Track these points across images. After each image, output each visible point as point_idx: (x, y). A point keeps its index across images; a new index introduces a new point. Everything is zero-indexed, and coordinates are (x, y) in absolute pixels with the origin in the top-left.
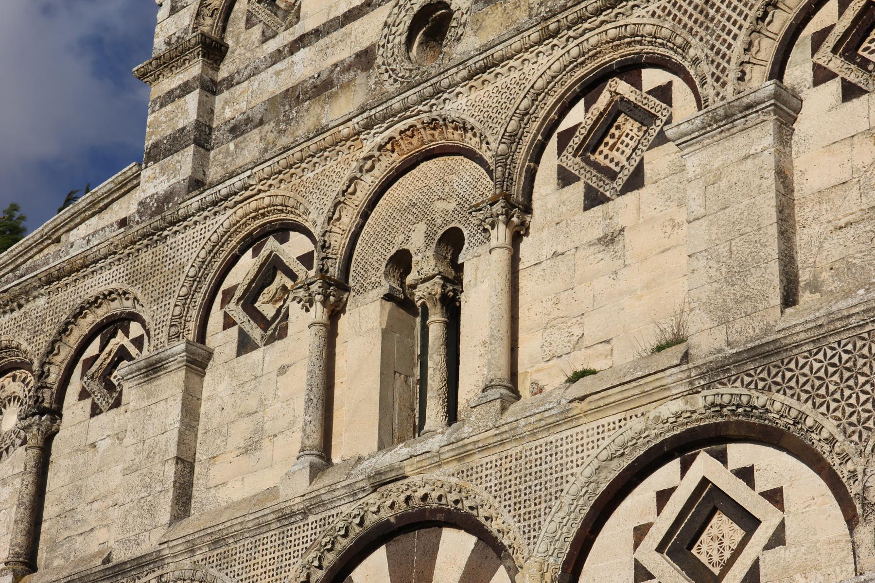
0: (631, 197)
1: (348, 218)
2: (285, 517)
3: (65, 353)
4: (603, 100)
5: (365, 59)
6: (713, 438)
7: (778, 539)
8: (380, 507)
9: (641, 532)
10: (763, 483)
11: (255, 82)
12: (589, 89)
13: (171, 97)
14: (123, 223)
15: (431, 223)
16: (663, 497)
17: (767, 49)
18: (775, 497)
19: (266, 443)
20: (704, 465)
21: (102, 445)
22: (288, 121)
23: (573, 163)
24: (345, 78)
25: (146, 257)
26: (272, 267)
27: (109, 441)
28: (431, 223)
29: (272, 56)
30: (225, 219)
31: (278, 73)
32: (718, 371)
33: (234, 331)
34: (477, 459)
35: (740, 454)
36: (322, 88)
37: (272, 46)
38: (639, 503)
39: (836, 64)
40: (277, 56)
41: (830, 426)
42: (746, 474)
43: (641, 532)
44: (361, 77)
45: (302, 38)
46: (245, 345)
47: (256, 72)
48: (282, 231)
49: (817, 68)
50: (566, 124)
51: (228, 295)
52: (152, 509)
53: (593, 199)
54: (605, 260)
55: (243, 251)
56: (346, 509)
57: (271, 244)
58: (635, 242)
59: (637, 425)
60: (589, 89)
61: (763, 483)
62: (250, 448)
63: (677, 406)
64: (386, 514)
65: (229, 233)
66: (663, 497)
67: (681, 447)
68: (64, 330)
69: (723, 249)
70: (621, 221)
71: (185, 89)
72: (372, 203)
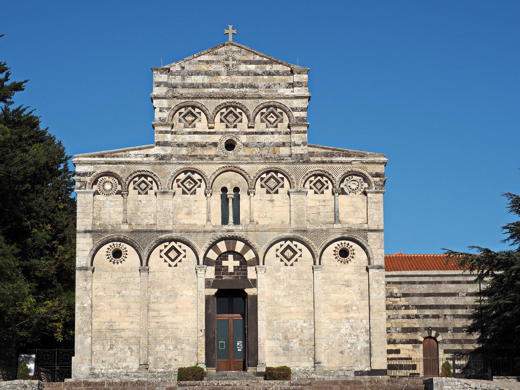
0: (275, 195)
1: (213, 177)
2: (205, 232)
3: (130, 178)
4: (270, 175)
5: (215, 144)
6: (292, 239)
7: (301, 256)
8: (227, 235)
9: (277, 250)
10: (298, 247)
11: (183, 136)
12: (268, 172)
13: (161, 132)
14: (147, 156)
15: (232, 184)
16: (281, 246)
17: (304, 181)
18: (301, 250)
19: (192, 214)
20: (288, 242)
21: (144, 202)
22: (195, 150)
23: (263, 184)
24: (210, 146)
25: (158, 167)
26: (189, 177)
27: (145, 202)
28: (232, 184)
29: (188, 132)
30: (181, 167)
31: (190, 137)
32: (295, 231)
33: (181, 189)
34: (249, 233)
35: (295, 243)
36: (203, 146)
37: (188, 130)
38: (277, 245)
39: (313, 187)
40: (190, 133)
41: (313, 244)
42: (296, 246)
43: (277, 250)
44: (214, 148)
45: (196, 132)
46: (184, 193)
47: (183, 134)
48: (193, 172)
49: (310, 187)
50: (262, 176)
51: (178, 181)
52: (167, 221)
53: (268, 192)
54: (271, 204)
55: (182, 172)
56: (220, 234)
57: (189, 174)
58: (277, 203)
59: (280, 235)
60: (268, 172)
61: (298, 247)
62: (189, 214)
63: (288, 234)
64: (227, 236)
65: (181, 169)
66: (281, 246)
67: (286, 240)
68: (131, 175)
69: (297, 212)
70: (274, 198)
71: (166, 132)
72: (218, 175)
